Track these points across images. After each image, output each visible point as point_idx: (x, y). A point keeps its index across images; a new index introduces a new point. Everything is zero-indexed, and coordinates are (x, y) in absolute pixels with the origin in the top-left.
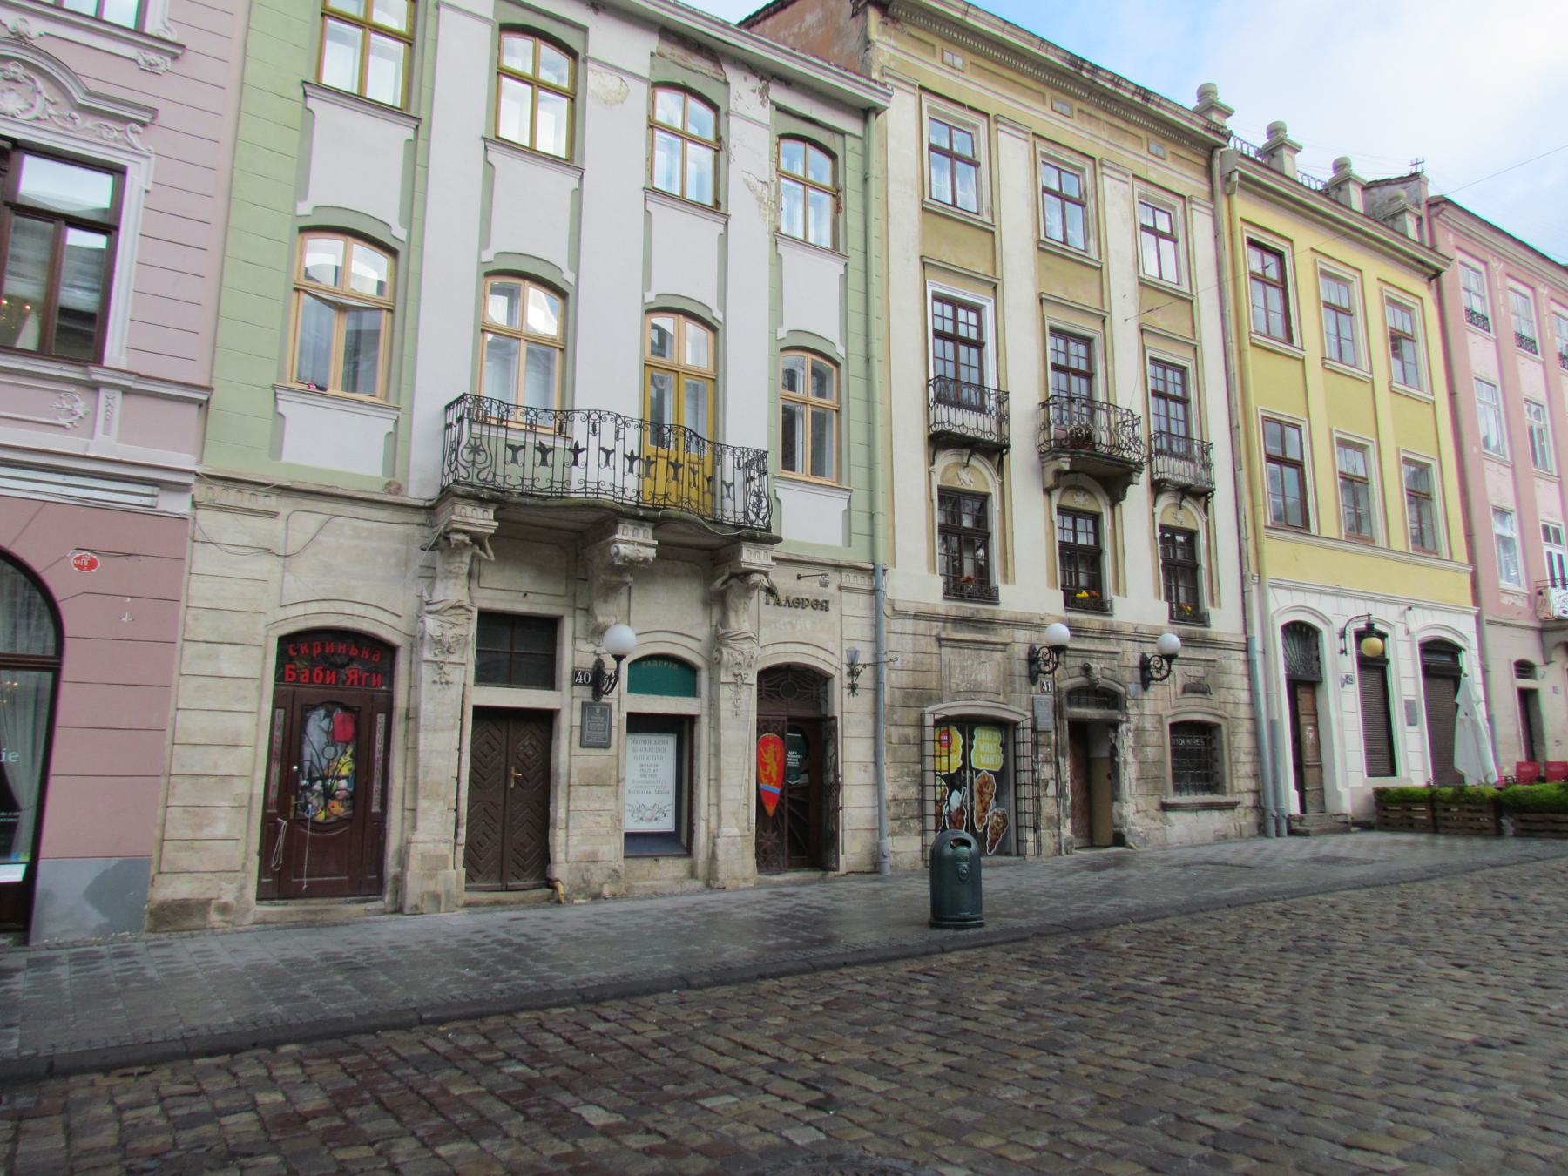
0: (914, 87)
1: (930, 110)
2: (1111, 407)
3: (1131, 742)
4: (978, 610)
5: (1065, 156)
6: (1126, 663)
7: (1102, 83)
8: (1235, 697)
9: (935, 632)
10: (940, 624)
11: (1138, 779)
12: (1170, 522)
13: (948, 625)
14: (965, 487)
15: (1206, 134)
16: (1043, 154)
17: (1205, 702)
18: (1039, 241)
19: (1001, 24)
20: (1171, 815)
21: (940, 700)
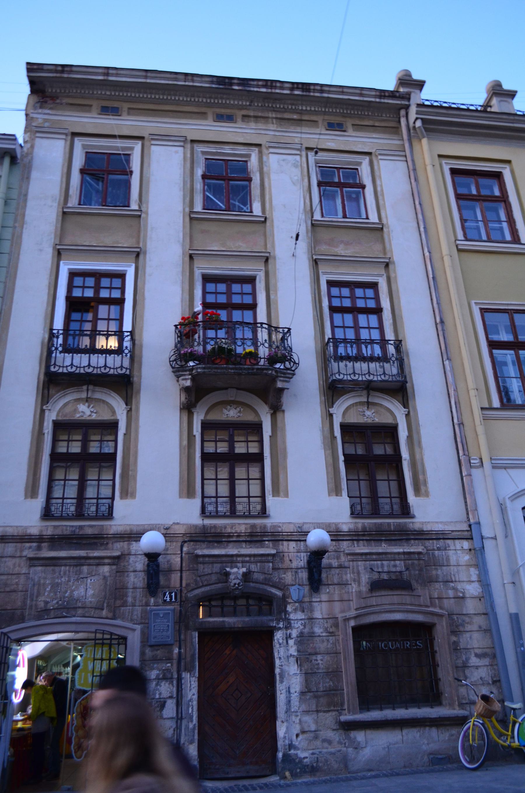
0: (66, 134)
1: (84, 146)
2: (271, 328)
3: (293, 651)
4: (81, 527)
5: (227, 149)
6: (287, 563)
7: (256, 89)
8: (455, 589)
9: (25, 553)
10: (35, 544)
11: (302, 693)
12: (354, 419)
13: (44, 545)
14: (86, 417)
15: (383, 101)
16: (204, 153)
17: (408, 600)
18: (191, 212)
19: (144, 74)
20: (360, 736)
21: (22, 619)
